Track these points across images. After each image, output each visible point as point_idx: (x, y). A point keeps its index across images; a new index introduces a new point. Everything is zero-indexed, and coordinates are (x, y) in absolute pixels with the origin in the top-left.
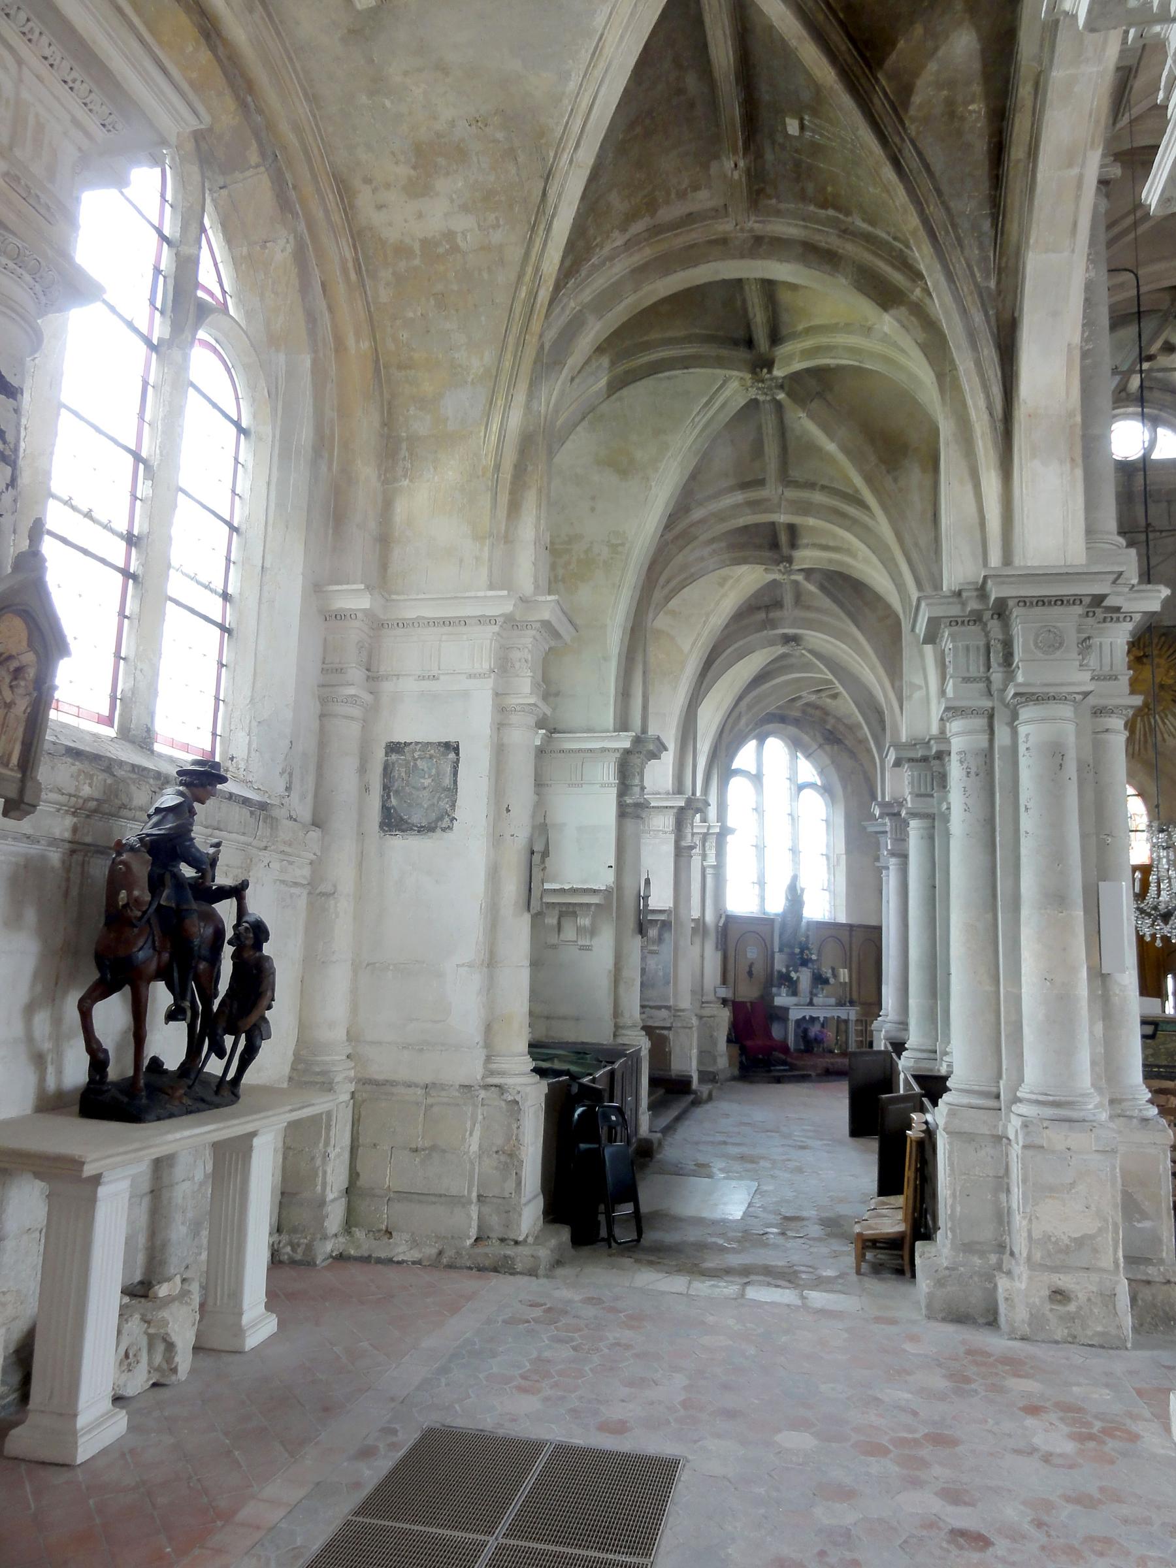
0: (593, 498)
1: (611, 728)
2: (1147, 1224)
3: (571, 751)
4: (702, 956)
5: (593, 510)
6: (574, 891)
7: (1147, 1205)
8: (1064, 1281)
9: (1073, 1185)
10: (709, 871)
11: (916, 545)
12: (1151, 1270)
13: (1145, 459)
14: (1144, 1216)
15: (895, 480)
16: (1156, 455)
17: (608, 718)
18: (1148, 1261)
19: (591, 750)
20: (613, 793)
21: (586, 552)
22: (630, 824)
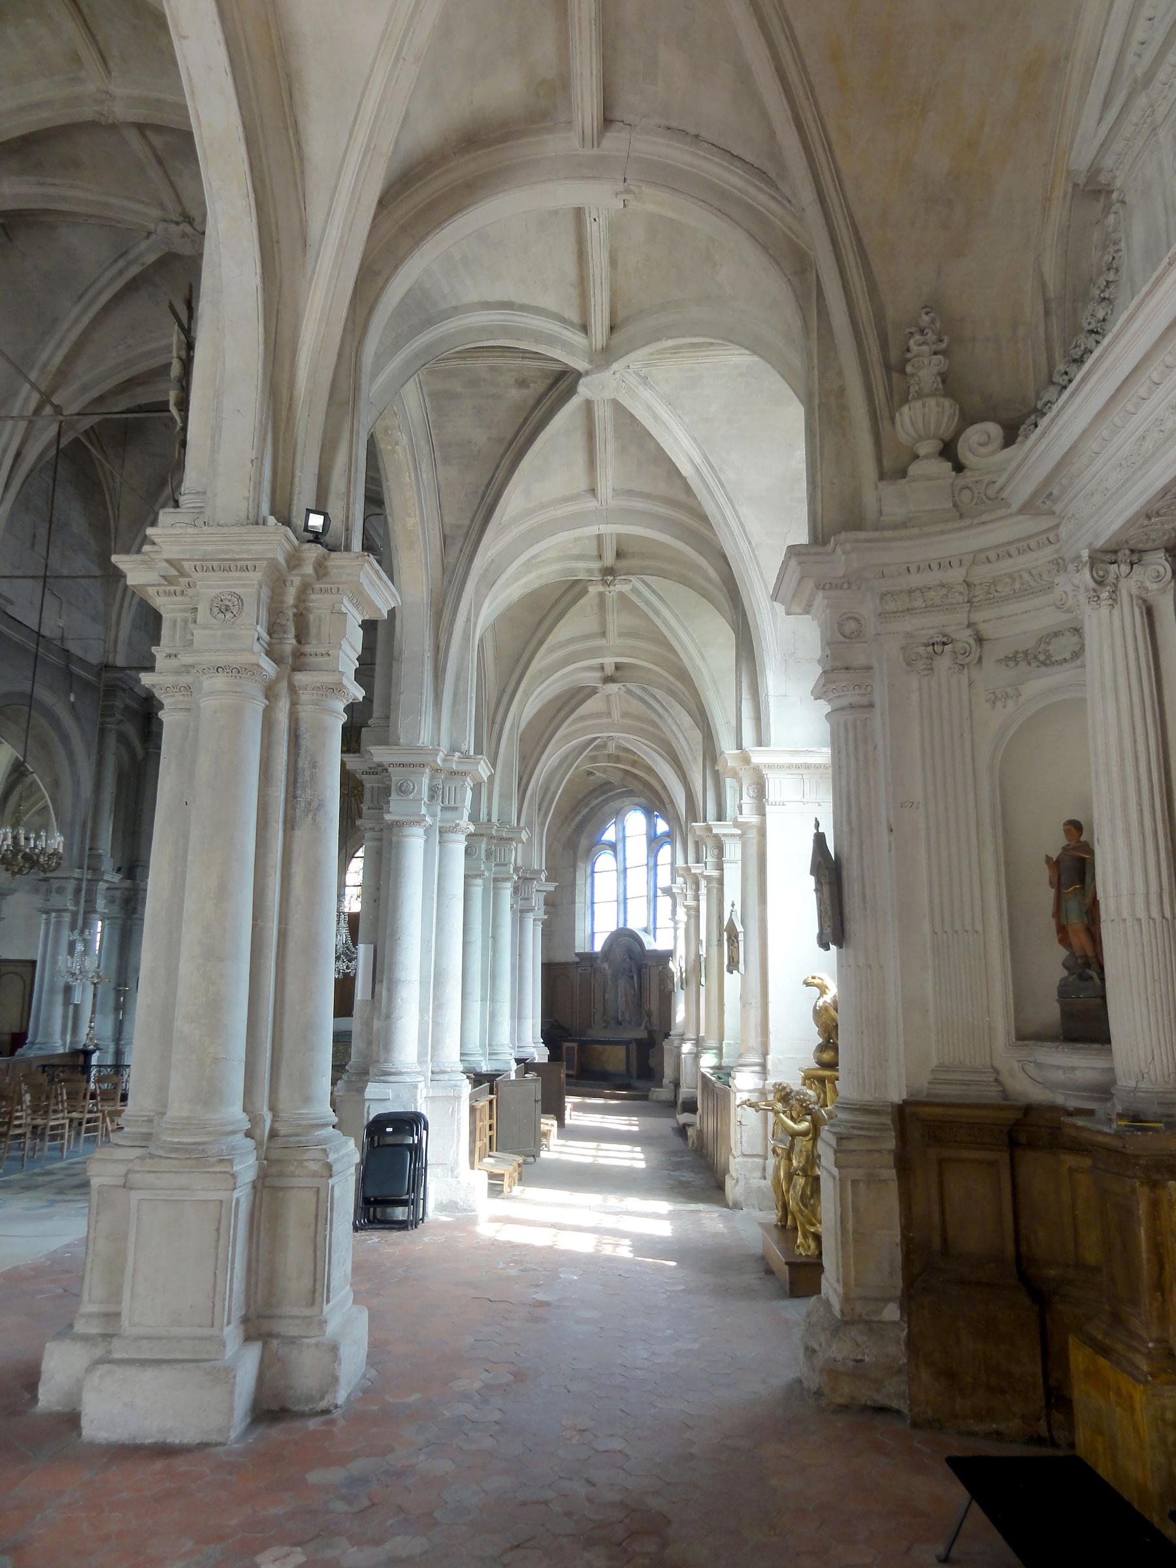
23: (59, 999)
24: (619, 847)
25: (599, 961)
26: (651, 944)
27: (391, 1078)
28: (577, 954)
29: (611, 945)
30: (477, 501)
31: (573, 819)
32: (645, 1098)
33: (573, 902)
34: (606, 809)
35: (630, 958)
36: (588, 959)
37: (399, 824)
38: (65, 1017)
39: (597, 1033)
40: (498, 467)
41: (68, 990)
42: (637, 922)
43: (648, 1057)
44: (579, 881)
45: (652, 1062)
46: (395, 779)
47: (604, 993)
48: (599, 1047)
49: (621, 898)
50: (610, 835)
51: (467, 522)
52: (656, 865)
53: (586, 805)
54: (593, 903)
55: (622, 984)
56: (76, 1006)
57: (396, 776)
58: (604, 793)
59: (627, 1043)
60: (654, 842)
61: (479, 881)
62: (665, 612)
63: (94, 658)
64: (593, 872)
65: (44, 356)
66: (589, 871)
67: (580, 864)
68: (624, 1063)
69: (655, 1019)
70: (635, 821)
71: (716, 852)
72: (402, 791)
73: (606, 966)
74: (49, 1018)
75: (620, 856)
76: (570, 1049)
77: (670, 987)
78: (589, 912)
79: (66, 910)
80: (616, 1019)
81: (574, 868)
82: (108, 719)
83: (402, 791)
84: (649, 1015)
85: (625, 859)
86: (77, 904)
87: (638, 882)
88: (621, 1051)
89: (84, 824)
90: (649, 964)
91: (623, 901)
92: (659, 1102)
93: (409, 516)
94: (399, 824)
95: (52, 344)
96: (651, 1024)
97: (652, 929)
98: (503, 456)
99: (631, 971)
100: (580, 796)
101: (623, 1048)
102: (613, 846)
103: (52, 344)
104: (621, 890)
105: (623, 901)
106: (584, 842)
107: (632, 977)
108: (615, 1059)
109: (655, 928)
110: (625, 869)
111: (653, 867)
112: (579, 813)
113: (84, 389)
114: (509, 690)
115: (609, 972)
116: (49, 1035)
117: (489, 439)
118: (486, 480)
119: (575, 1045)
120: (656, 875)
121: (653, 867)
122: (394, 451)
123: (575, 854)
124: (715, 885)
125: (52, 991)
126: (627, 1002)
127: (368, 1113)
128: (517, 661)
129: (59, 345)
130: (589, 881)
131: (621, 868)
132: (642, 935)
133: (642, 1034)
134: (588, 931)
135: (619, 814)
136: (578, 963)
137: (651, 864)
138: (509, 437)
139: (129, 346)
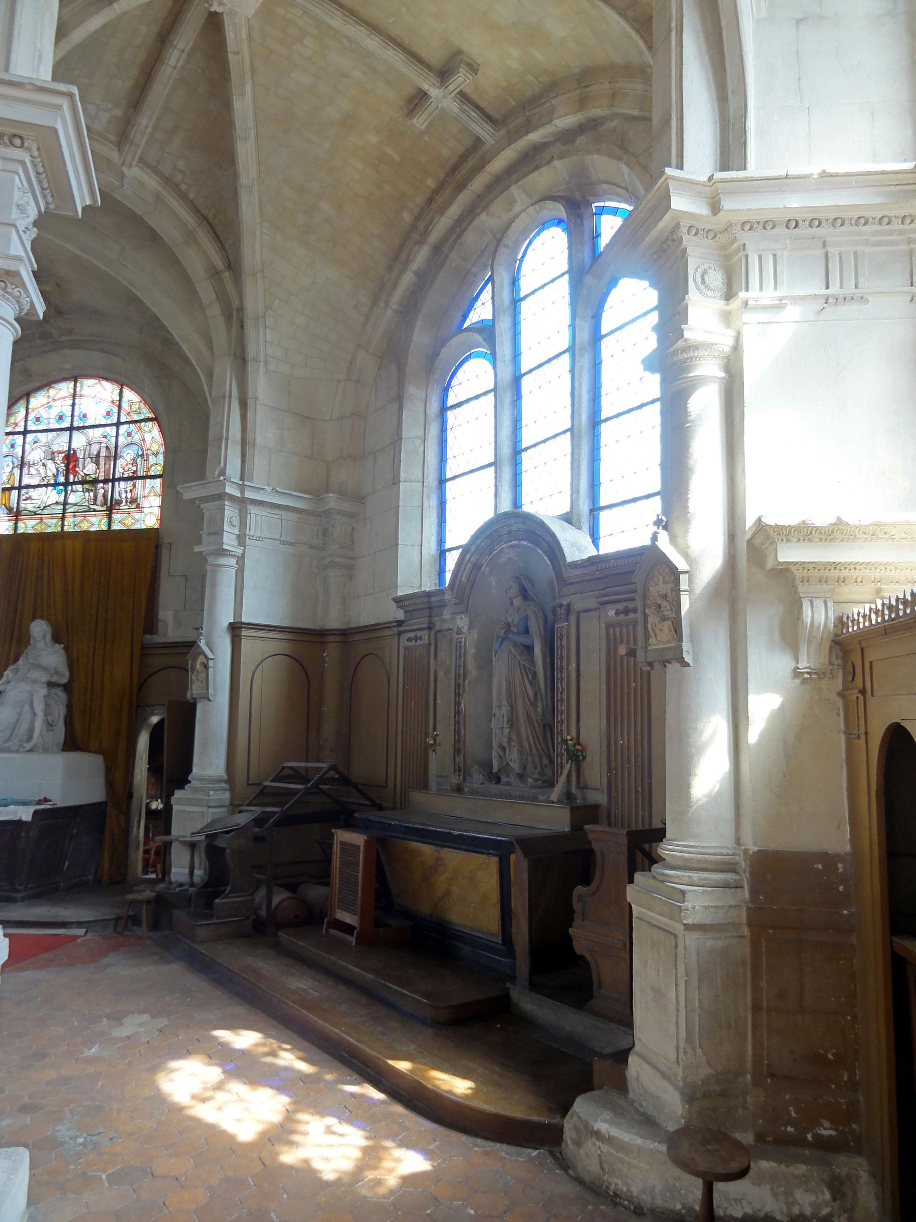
24: (503, 327)
25: (446, 615)
26: (576, 546)
28: (399, 601)
29: (477, 567)
31: (395, 285)
32: (542, 1137)
33: (395, 481)
34: (469, 237)
35: (524, 594)
36: (423, 606)
39: (437, 805)
42: (546, 494)
43: (568, 916)
44: (410, 430)
45: (583, 936)
47: (458, 694)
48: (427, 850)
49: (506, 450)
50: (482, 311)
52: (596, 338)
53: (421, 242)
54: (442, 481)
55: (501, 667)
58: (461, 187)
59: (501, 850)
60: (589, 280)
64: (444, 409)
66: (434, 407)
67: (411, 390)
68: (495, 913)
69: (595, 770)
70: (546, 254)
73: (462, 622)
75: (504, 349)
76: (347, 848)
77: (660, 639)
78: (432, 503)
80: (486, 765)
81: (399, 400)
84: (577, 757)
85: (516, 355)
87: (548, 402)
88: (484, 872)
90: (578, 606)
91: (510, 459)
92: (615, 1199)
96: (583, 787)
97: (589, 511)
99: (527, 631)
100: (407, 217)
101: (493, 863)
102: (487, 331)
104: (506, 431)
105: (510, 459)
106: (420, 338)
107: (529, 649)
108: (471, 893)
109: (595, 510)
110: (517, 380)
111: (586, 348)
112: (407, 262)
115: (471, 640)
119: (358, 839)
120: (596, 365)
121: (586, 348)
123: (401, 366)
126: (512, 723)
130: (434, 430)
131: (506, 374)
132: (557, 528)
133: (552, 818)
134: (431, 547)
135: (499, 251)
136: (400, 623)
137: (584, 335)
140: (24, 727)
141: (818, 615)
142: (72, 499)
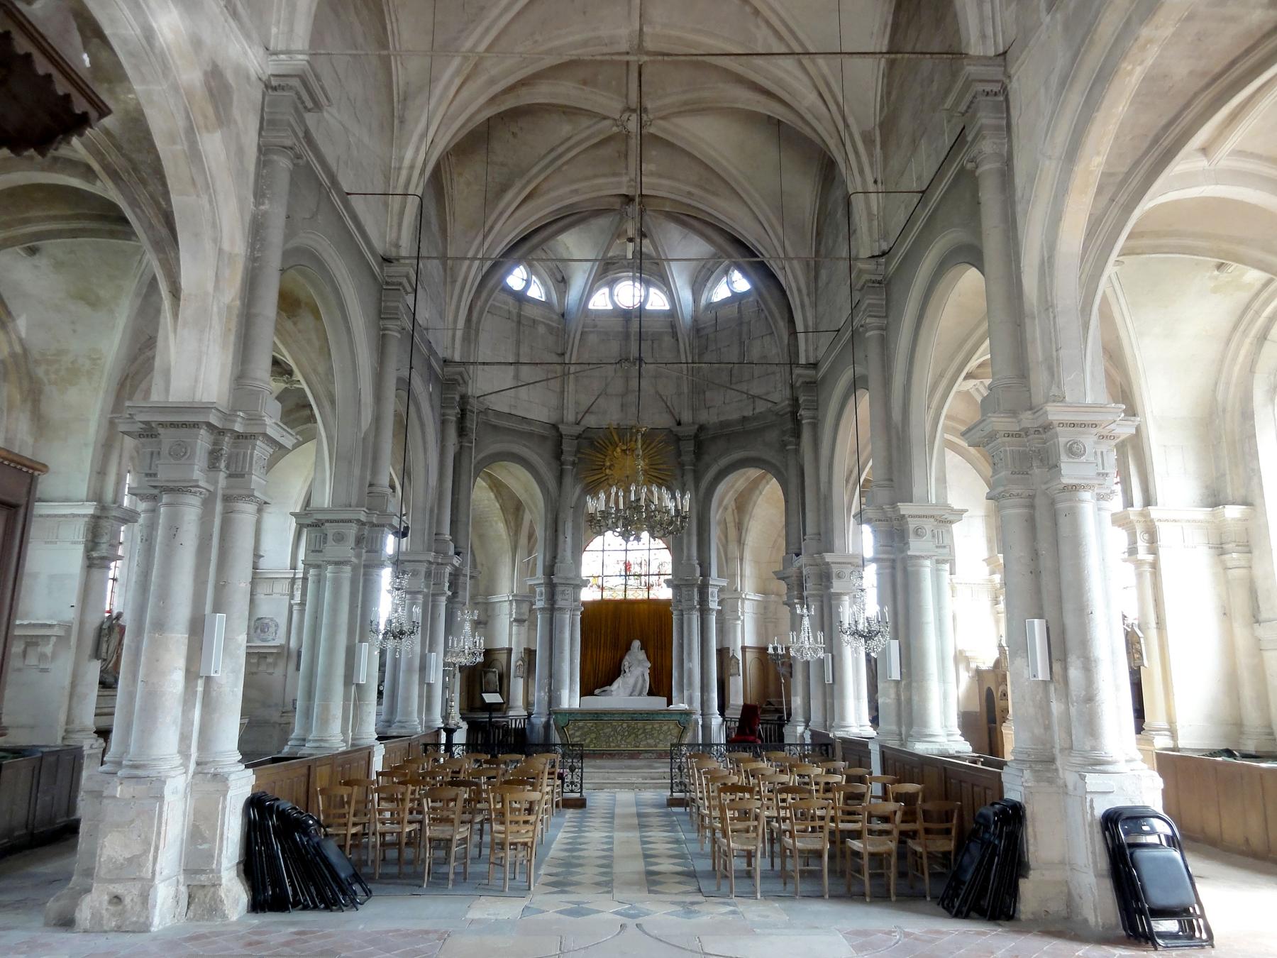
0: (73, 323)
1: (84, 495)
2: (205, 846)
3: (48, 516)
4: (285, 676)
5: (74, 331)
6: (35, 626)
7: (207, 834)
8: (118, 889)
9: (132, 821)
10: (295, 607)
11: (315, 370)
12: (203, 877)
13: (641, 308)
14: (204, 840)
15: (295, 324)
16: (648, 307)
17: (82, 490)
18: (203, 872)
19: (64, 516)
20: (79, 550)
21: (72, 363)
22: (96, 573)
23: (416, 678)
27: (1109, 768)
30: (1145, 146)
37: (1075, 488)
38: (420, 696)
40: (1188, 105)
41: (423, 668)
46: (1062, 440)
51: (1125, 169)
56: (429, 685)
57: (1063, 437)
61: (928, 562)
62: (1122, 300)
63: (442, 353)
65: (468, 44)
71: (1146, 536)
72: (1074, 451)
74: (407, 699)
79: (419, 592)
82: (449, 411)
83: (1074, 451)
86: (428, 586)
89: (432, 511)
93: (1098, 154)
94: (1075, 488)
95: (480, 30)
98: (1196, 95)
103: (480, 30)
113: (492, 81)
114: (948, 375)
116: (407, 713)
117: (1191, 73)
118: (1164, 121)
122: (1130, 73)
124: (1147, 569)
125: (409, 670)
127: (1092, 807)
128: (960, 346)
129: (487, 30)
138: (1218, 69)
139: (536, 42)
140: (639, 686)
141: (973, 666)
142: (629, 582)
